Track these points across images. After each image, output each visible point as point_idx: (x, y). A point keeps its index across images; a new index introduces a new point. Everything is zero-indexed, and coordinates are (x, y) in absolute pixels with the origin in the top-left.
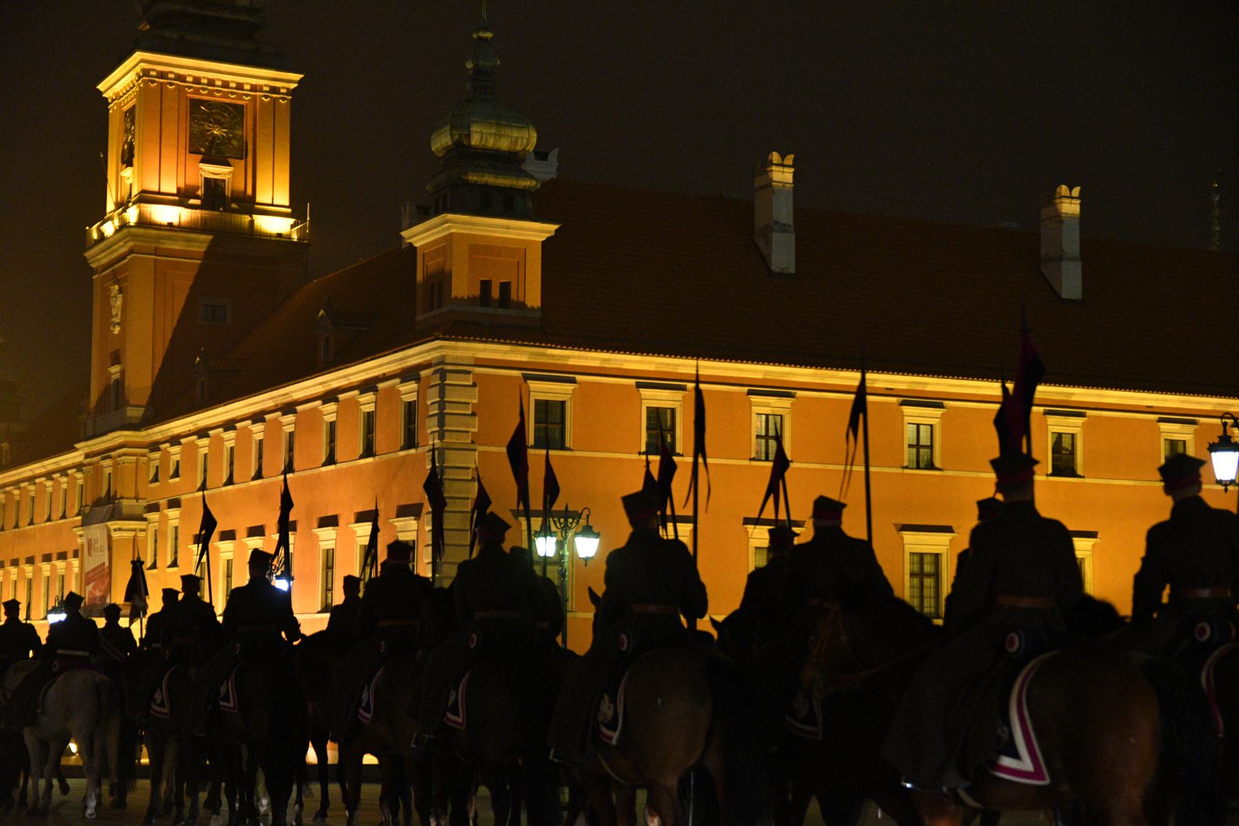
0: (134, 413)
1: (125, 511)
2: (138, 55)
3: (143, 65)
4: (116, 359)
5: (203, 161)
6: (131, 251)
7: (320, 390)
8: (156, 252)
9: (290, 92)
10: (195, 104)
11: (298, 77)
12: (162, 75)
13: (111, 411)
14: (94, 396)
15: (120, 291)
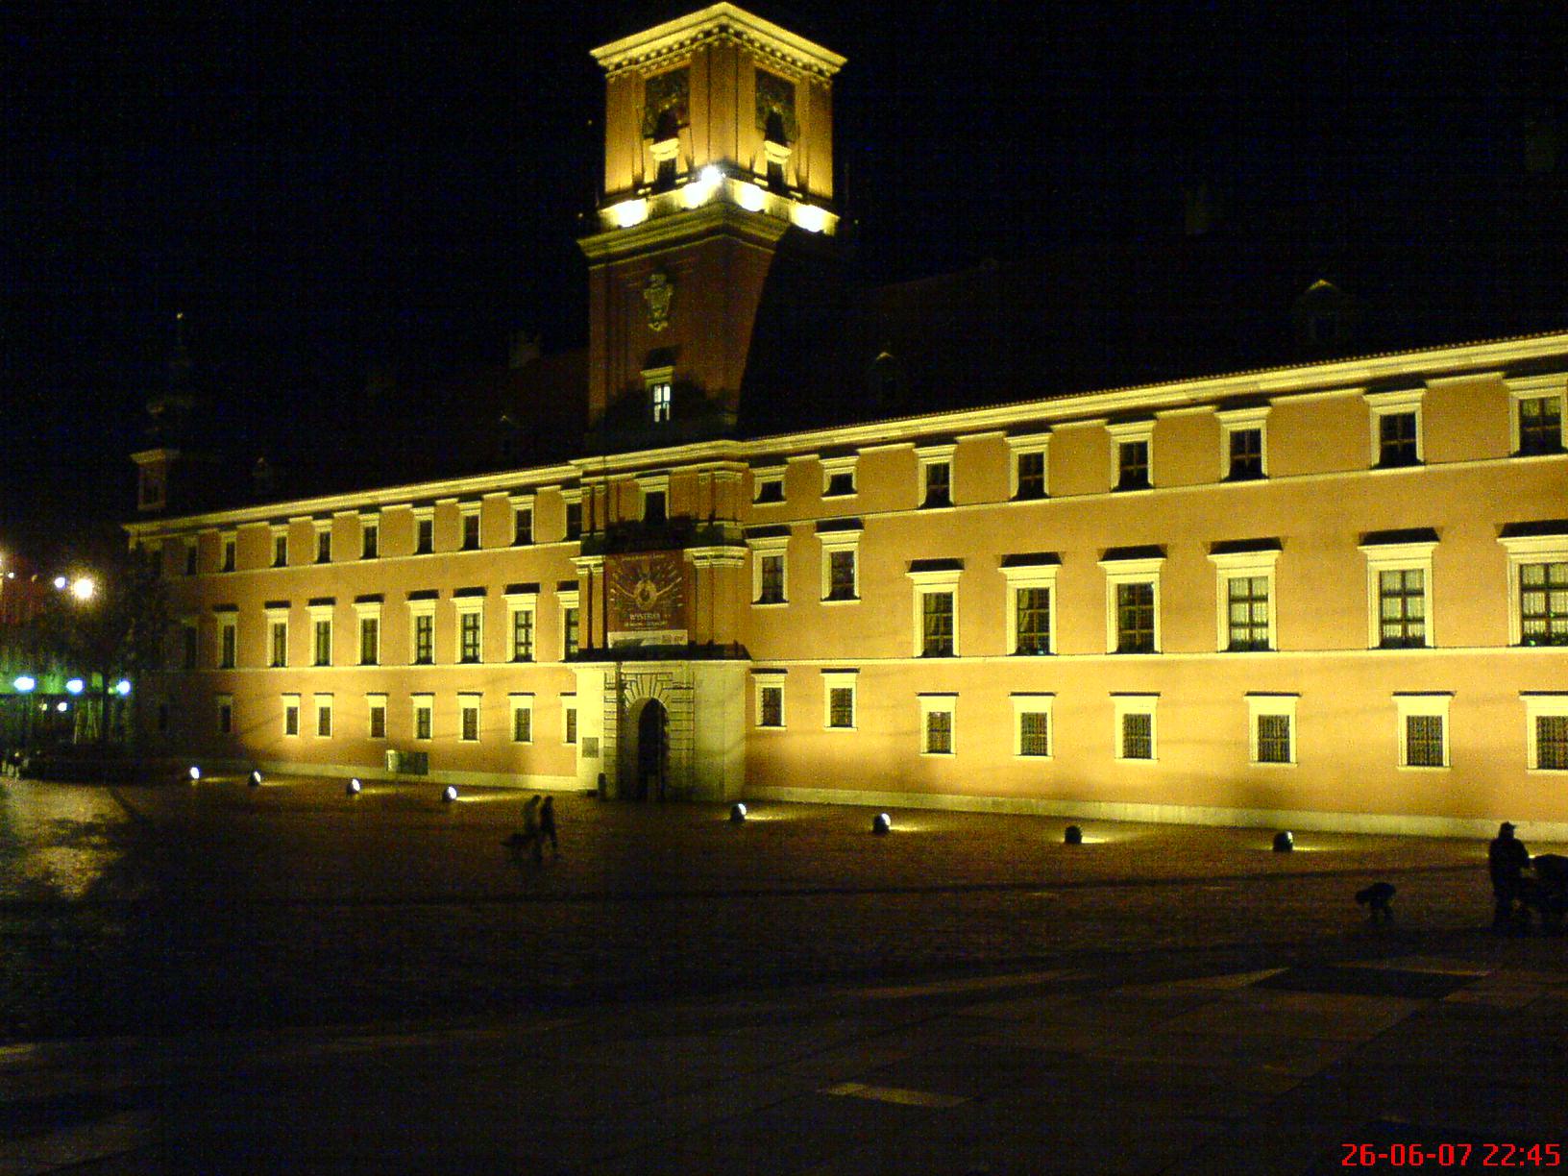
0: (731, 420)
1: (727, 535)
2: (724, 4)
3: (724, 20)
4: (656, 360)
5: (767, 138)
6: (710, 232)
7: (1366, 374)
8: (737, 233)
9: (834, 77)
10: (762, 76)
11: (841, 60)
12: (738, 34)
13: (629, 425)
14: (597, 401)
15: (667, 281)
